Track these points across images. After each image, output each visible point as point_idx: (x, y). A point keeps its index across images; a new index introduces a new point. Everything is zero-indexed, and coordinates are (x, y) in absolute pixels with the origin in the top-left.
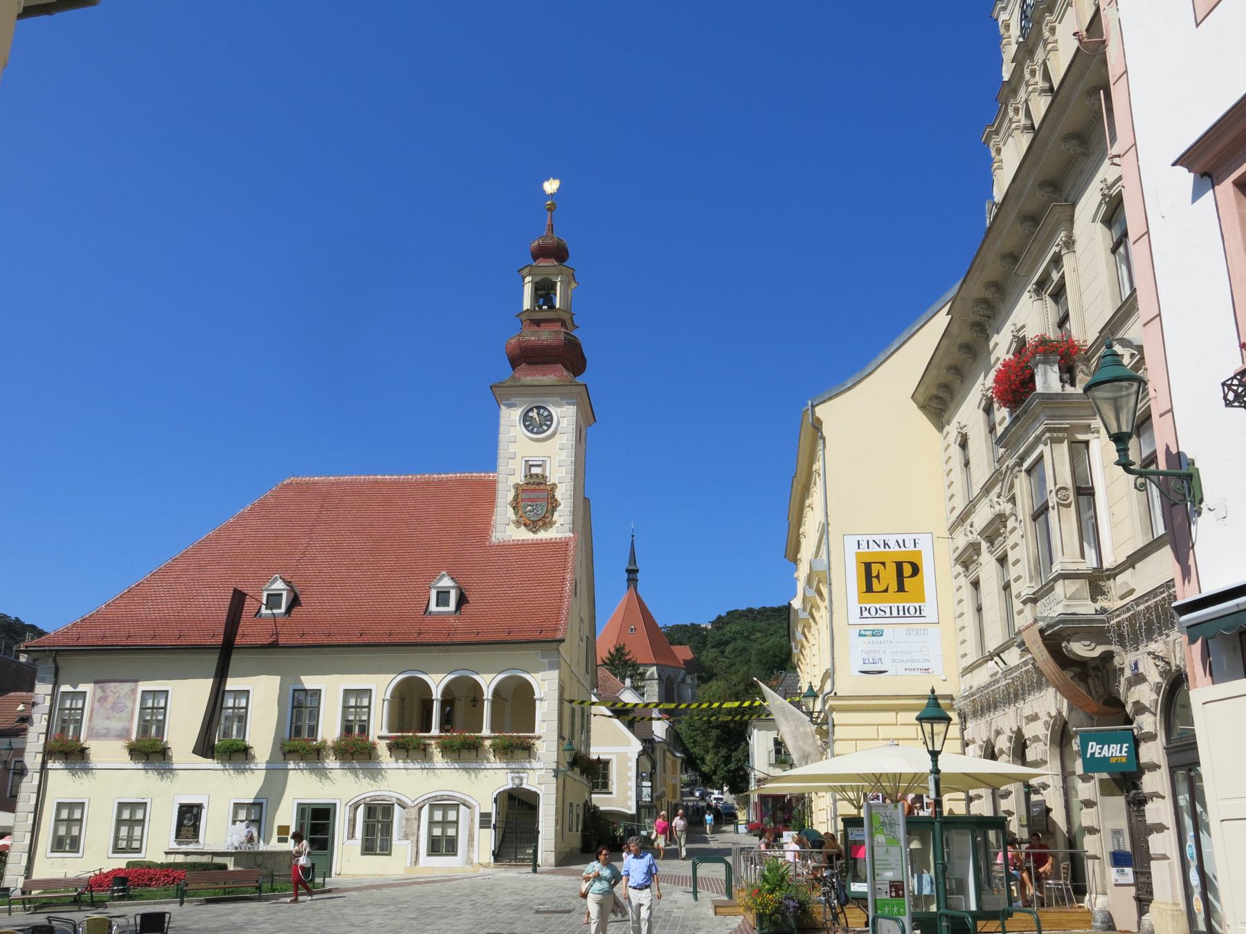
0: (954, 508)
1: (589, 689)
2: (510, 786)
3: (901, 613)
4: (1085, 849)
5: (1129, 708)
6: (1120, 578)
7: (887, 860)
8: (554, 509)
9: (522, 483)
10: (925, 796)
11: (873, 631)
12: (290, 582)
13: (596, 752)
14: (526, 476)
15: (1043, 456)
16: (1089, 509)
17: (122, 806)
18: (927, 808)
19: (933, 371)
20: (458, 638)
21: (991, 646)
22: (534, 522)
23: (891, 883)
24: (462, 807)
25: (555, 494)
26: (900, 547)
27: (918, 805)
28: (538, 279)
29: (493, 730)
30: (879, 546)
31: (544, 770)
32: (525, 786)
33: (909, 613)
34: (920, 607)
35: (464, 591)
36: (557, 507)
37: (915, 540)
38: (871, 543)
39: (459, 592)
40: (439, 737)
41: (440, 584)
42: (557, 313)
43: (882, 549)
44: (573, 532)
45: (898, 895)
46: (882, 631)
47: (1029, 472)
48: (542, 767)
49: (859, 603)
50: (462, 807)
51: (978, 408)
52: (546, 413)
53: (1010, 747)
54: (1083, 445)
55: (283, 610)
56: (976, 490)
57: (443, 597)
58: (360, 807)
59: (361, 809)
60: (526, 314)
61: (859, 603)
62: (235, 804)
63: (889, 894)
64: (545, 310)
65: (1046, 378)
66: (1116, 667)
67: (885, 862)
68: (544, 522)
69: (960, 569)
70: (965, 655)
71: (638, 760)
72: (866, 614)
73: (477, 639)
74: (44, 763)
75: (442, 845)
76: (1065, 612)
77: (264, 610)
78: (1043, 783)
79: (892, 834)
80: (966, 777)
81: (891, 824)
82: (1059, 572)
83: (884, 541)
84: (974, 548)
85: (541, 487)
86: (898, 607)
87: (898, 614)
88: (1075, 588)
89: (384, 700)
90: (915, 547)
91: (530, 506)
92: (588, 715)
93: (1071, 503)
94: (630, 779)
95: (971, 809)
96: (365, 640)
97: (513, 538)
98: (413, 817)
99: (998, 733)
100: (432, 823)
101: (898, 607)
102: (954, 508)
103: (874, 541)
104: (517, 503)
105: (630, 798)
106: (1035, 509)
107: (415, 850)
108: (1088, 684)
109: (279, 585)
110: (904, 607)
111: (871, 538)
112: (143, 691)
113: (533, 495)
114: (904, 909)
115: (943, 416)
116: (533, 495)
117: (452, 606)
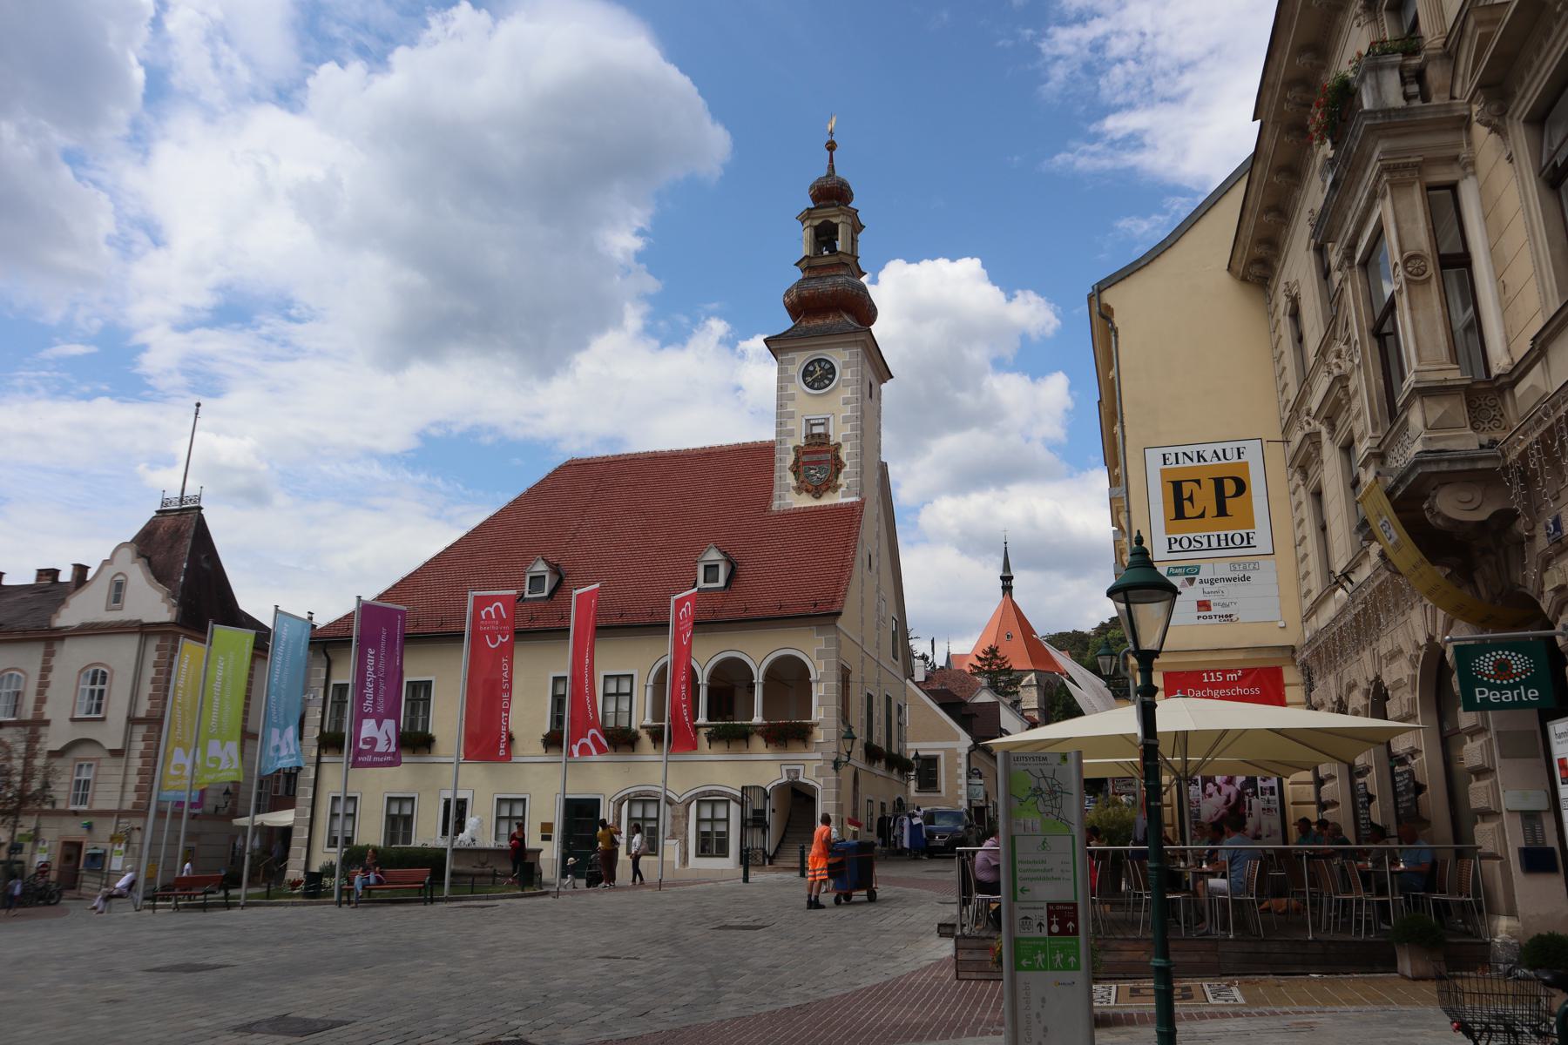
0: (1288, 401)
1: (903, 679)
2: (785, 779)
3: (1223, 544)
4: (1478, 843)
5: (1545, 605)
6: (1520, 389)
7: (1044, 862)
8: (838, 471)
9: (803, 445)
10: (1259, 778)
11: (1187, 567)
12: (557, 565)
13: (914, 747)
14: (806, 437)
15: (1382, 229)
16: (1465, 309)
17: (390, 799)
18: (1262, 795)
19: (1251, 222)
20: (724, 616)
21: (1339, 567)
22: (816, 487)
23: (1051, 908)
24: (731, 802)
25: (840, 454)
26: (1219, 459)
27: (1250, 790)
28: (816, 223)
29: (765, 717)
30: (1192, 460)
31: (822, 762)
32: (801, 779)
33: (1234, 543)
34: (1248, 534)
35: (736, 565)
36: (841, 468)
37: (1238, 449)
38: (1180, 456)
39: (730, 567)
40: (705, 726)
41: (705, 559)
42: (841, 256)
43: (1195, 463)
44: (860, 495)
45: (1064, 931)
46: (1198, 567)
47: (1365, 264)
48: (820, 757)
49: (1167, 534)
50: (732, 804)
51: (1308, 249)
52: (827, 366)
53: (1368, 704)
54: (1448, 192)
55: (546, 594)
56: (1311, 360)
57: (711, 570)
58: (692, 804)
59: (626, 803)
60: (806, 261)
61: (1167, 534)
62: (498, 799)
63: (1045, 930)
64: (826, 256)
65: (1379, 92)
66: (1521, 534)
67: (1041, 867)
68: (829, 485)
69: (1297, 478)
70: (1309, 592)
71: (969, 756)
72: (1176, 547)
73: (744, 616)
74: (319, 756)
75: (711, 845)
76: (1425, 449)
77: (527, 595)
78: (1412, 747)
79: (1056, 811)
80: (1271, 733)
81: (1052, 792)
82: (1412, 386)
83: (1198, 452)
84: (1313, 439)
85: (825, 448)
86: (1218, 536)
87: (1219, 545)
88: (1443, 411)
89: (646, 686)
90: (1239, 458)
91: (813, 469)
92: (900, 708)
93: (1430, 277)
94: (960, 776)
95: (1322, 794)
96: (625, 621)
97: (794, 506)
98: (680, 814)
99: (1352, 687)
100: (699, 820)
101: (1218, 536)
102: (1288, 401)
103: (1184, 453)
104: (798, 467)
105: (960, 797)
106: (1377, 319)
107: (683, 850)
108: (1474, 582)
109: (541, 567)
110: (1226, 535)
111: (1180, 450)
112: (408, 682)
113: (815, 458)
114: (1077, 957)
115: (1269, 287)
116: (815, 458)
117: (721, 583)
